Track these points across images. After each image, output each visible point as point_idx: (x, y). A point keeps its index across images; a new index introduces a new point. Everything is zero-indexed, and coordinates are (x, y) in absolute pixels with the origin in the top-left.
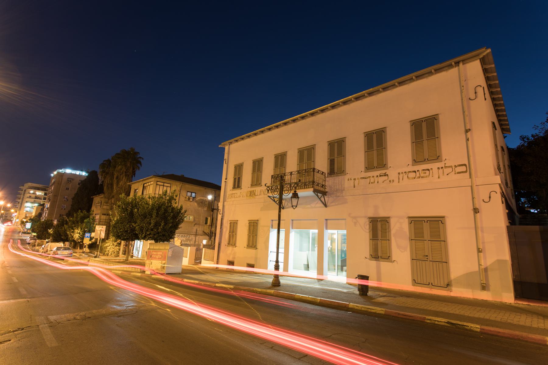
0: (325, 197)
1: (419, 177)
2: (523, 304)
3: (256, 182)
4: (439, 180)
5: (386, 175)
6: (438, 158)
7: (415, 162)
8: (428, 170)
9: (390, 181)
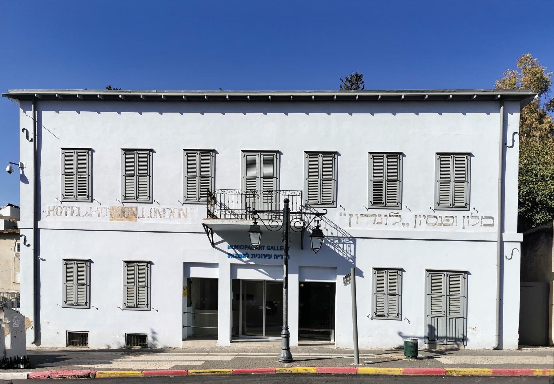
1: (441, 225)
4: (463, 231)
5: (397, 216)
8: (452, 217)
9: (403, 224)
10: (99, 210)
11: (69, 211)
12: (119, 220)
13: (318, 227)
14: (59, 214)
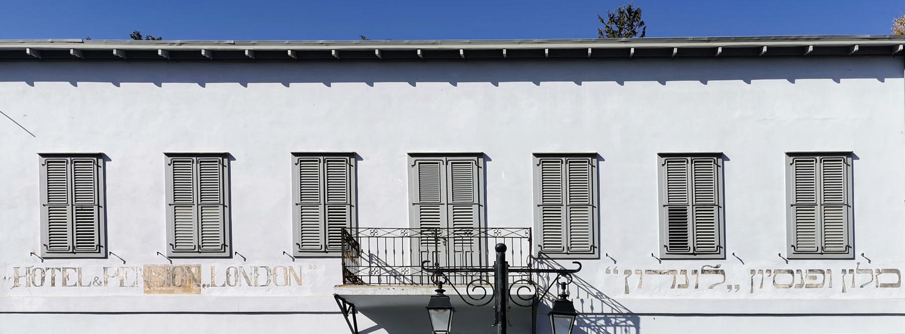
1: (801, 286)
4: (844, 297)
8: (822, 272)
9: (730, 287)
10: (122, 274)
11: (59, 276)
12: (164, 292)
13: (564, 296)
14: (38, 282)
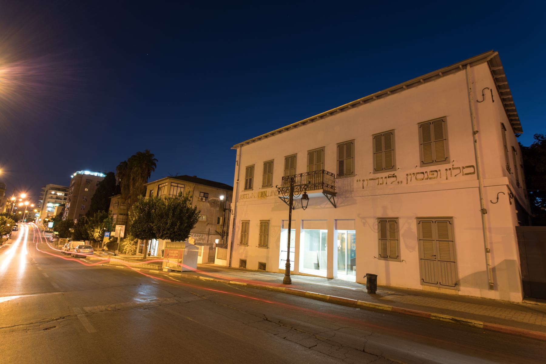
0: (335, 198)
1: (427, 179)
2: (531, 303)
3: (267, 183)
5: (394, 176)
6: (445, 160)
7: (423, 163)
8: (436, 171)
9: (398, 182)
